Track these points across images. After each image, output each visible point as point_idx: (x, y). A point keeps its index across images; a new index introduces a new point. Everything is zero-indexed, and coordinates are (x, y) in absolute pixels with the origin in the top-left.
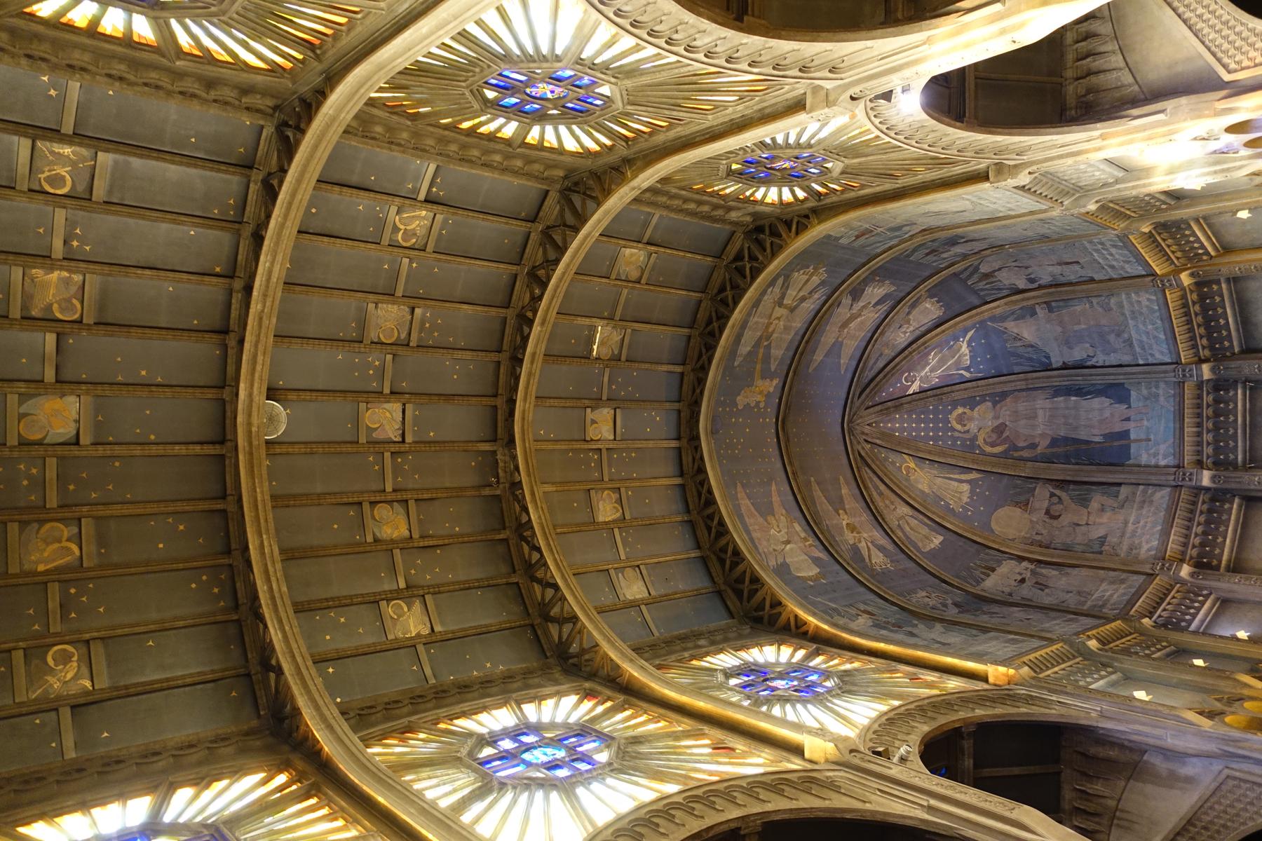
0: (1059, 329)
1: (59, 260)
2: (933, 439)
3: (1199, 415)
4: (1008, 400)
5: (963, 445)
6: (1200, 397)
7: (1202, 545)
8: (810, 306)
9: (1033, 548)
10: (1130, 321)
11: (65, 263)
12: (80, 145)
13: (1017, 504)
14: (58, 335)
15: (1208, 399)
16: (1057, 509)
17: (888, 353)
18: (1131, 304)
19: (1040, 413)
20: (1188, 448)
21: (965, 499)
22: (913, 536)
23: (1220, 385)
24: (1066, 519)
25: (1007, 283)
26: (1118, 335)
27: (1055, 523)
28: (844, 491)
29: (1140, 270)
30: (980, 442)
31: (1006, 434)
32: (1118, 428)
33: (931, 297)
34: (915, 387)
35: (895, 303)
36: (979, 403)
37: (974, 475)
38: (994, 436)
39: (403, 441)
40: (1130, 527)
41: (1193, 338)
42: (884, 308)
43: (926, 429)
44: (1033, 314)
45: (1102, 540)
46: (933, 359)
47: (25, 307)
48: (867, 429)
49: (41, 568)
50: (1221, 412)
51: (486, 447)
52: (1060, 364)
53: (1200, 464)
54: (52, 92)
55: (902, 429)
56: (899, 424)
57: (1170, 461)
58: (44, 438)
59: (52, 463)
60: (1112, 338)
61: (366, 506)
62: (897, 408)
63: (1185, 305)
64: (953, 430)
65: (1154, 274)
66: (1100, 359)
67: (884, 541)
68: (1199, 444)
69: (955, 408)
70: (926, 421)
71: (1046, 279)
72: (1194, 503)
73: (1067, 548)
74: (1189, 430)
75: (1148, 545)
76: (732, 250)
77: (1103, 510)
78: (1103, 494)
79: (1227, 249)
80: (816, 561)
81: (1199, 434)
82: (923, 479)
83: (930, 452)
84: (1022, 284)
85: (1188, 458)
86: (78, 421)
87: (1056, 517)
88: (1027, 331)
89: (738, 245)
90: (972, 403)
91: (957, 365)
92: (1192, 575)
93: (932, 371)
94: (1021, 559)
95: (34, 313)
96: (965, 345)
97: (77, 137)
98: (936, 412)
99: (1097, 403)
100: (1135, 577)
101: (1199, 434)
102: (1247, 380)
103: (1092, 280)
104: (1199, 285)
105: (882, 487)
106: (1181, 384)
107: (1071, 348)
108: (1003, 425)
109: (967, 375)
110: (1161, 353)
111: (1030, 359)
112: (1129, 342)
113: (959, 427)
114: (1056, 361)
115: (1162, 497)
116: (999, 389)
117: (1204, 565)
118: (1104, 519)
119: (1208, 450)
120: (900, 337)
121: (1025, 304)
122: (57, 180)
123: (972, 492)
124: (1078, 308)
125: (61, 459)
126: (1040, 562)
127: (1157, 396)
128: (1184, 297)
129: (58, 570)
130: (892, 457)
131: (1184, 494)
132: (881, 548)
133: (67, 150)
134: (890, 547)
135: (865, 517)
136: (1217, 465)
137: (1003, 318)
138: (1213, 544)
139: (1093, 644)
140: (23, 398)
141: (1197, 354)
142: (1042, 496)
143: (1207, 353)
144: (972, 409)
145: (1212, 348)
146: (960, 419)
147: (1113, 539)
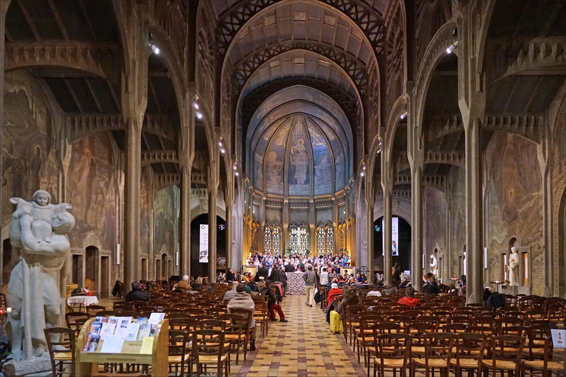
0: (324, 169)
2: (295, 135)
3: (301, 199)
4: (306, 154)
5: (293, 142)
6: (306, 200)
7: (271, 201)
8: (333, 113)
9: (266, 163)
10: (324, 186)
13: (277, 158)
15: (305, 201)
16: (277, 168)
17: (320, 125)
18: (329, 186)
19: (302, 163)
20: (293, 197)
21: (278, 144)
22: (267, 133)
23: (308, 204)
24: (274, 171)
25: (337, 158)
26: (322, 183)
27: (273, 168)
28: (280, 115)
29: (336, 190)
30: (294, 147)
31: (296, 154)
32: (298, 182)
33: (335, 139)
34: (310, 130)
35: (334, 131)
36: (305, 147)
37: (285, 146)
38: (296, 151)
39: (294, 21)
40: (274, 186)
41: (320, 199)
42: (333, 127)
43: (298, 135)
44: (329, 163)
45: (270, 180)
46: (318, 135)
48: (298, 118)
50: (302, 204)
51: (293, 38)
52: (315, 168)
53: (290, 200)
55: (298, 126)
56: (299, 127)
57: (290, 194)
60: (321, 181)
61: (275, 16)
62: (304, 126)
63: (327, 198)
64: (298, 140)
65: (335, 192)
66: (316, 178)
67: (266, 127)
68: (294, 199)
69: (304, 140)
70: (300, 133)
71: (337, 168)
72: (280, 199)
73: (267, 171)
74: (298, 198)
75: (269, 190)
76: (349, 97)
77: (277, 179)
78: (281, 179)
79: (339, 207)
80: (261, 116)
81: (297, 199)
82: (283, 133)
83: (291, 134)
84: (337, 161)
85: (291, 197)
87: (274, 168)
88: (324, 161)
89: (351, 99)
90: (305, 145)
91: (316, 142)
92: (264, 200)
93: (315, 135)
94: (263, 161)
96: (321, 144)
98: (303, 135)
99: (305, 178)
100: (262, 188)
101: (297, 199)
102: (309, 209)
103: (335, 178)
104: (332, 201)
105: (281, 123)
106: (309, 196)
107: (319, 171)
108: (299, 153)
109: (313, 144)
110: (316, 192)
111: (317, 160)
112: (320, 185)
113: (298, 141)
114: (316, 167)
115: (282, 192)
116: (309, 152)
117: (266, 202)
118: (275, 180)
119: (293, 201)
120: (325, 128)
121: (331, 161)
123: (280, 146)
124: (329, 174)
126: (263, 165)
127: (306, 190)
128: (329, 198)
130: (289, 124)
131: (282, 197)
132: (264, 128)
134: (265, 129)
135: (272, 121)
136: (289, 203)
137: (328, 155)
138: (271, 203)
139: (250, 187)
141: (316, 199)
142: (280, 164)
143: (316, 201)
144: (303, 145)
145: (317, 202)
146: (301, 142)
147: (270, 181)
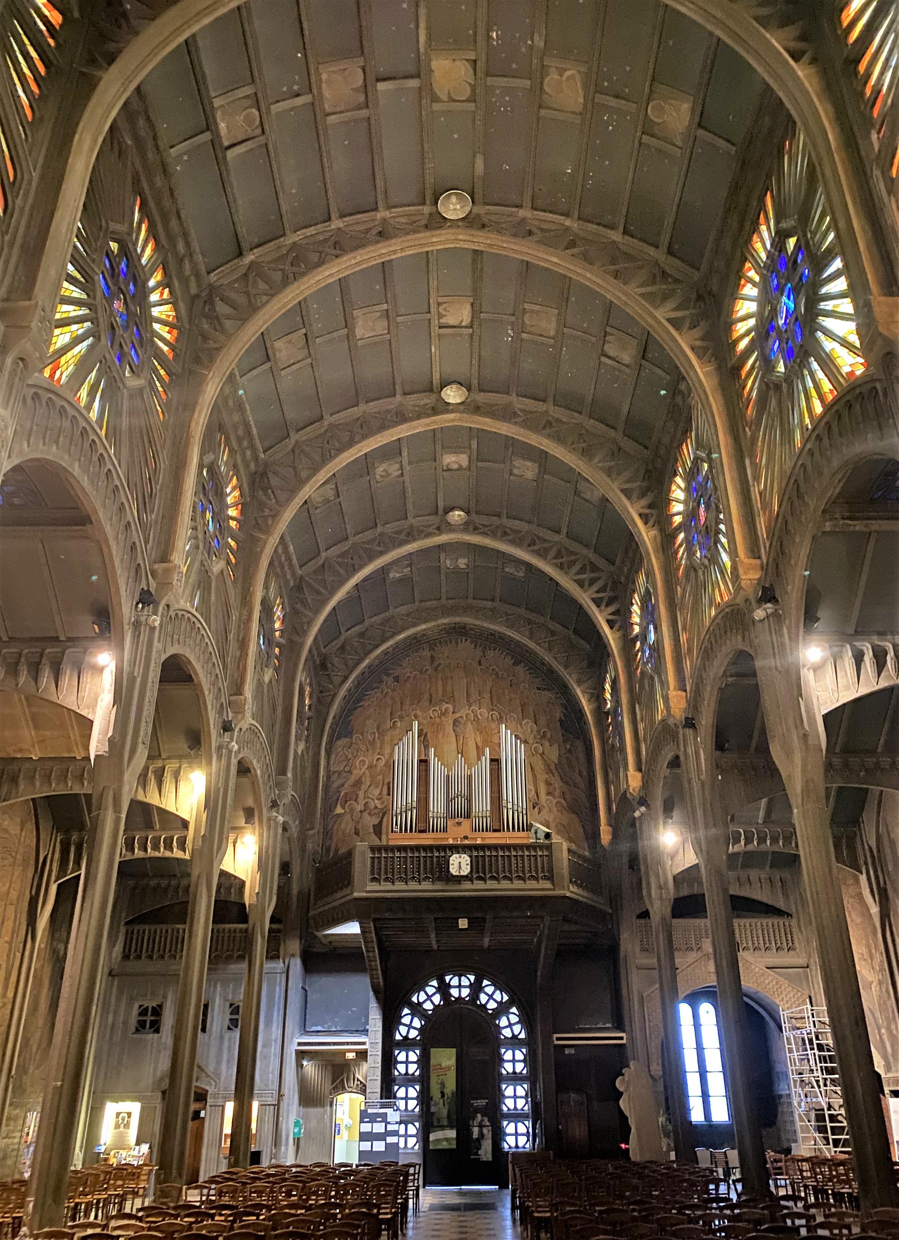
1: (314, 96)
11: (315, 91)
12: (214, 118)
14: (378, 80)
47: (359, 108)
49: (581, 100)
54: (185, 158)
58: (470, 84)
59: (490, 81)
86: (454, 60)
95: (362, 98)
97: (209, 126)
122: (249, 120)
125: (488, 74)
129: (586, 88)
133: (222, 126)
140: (435, 99)
